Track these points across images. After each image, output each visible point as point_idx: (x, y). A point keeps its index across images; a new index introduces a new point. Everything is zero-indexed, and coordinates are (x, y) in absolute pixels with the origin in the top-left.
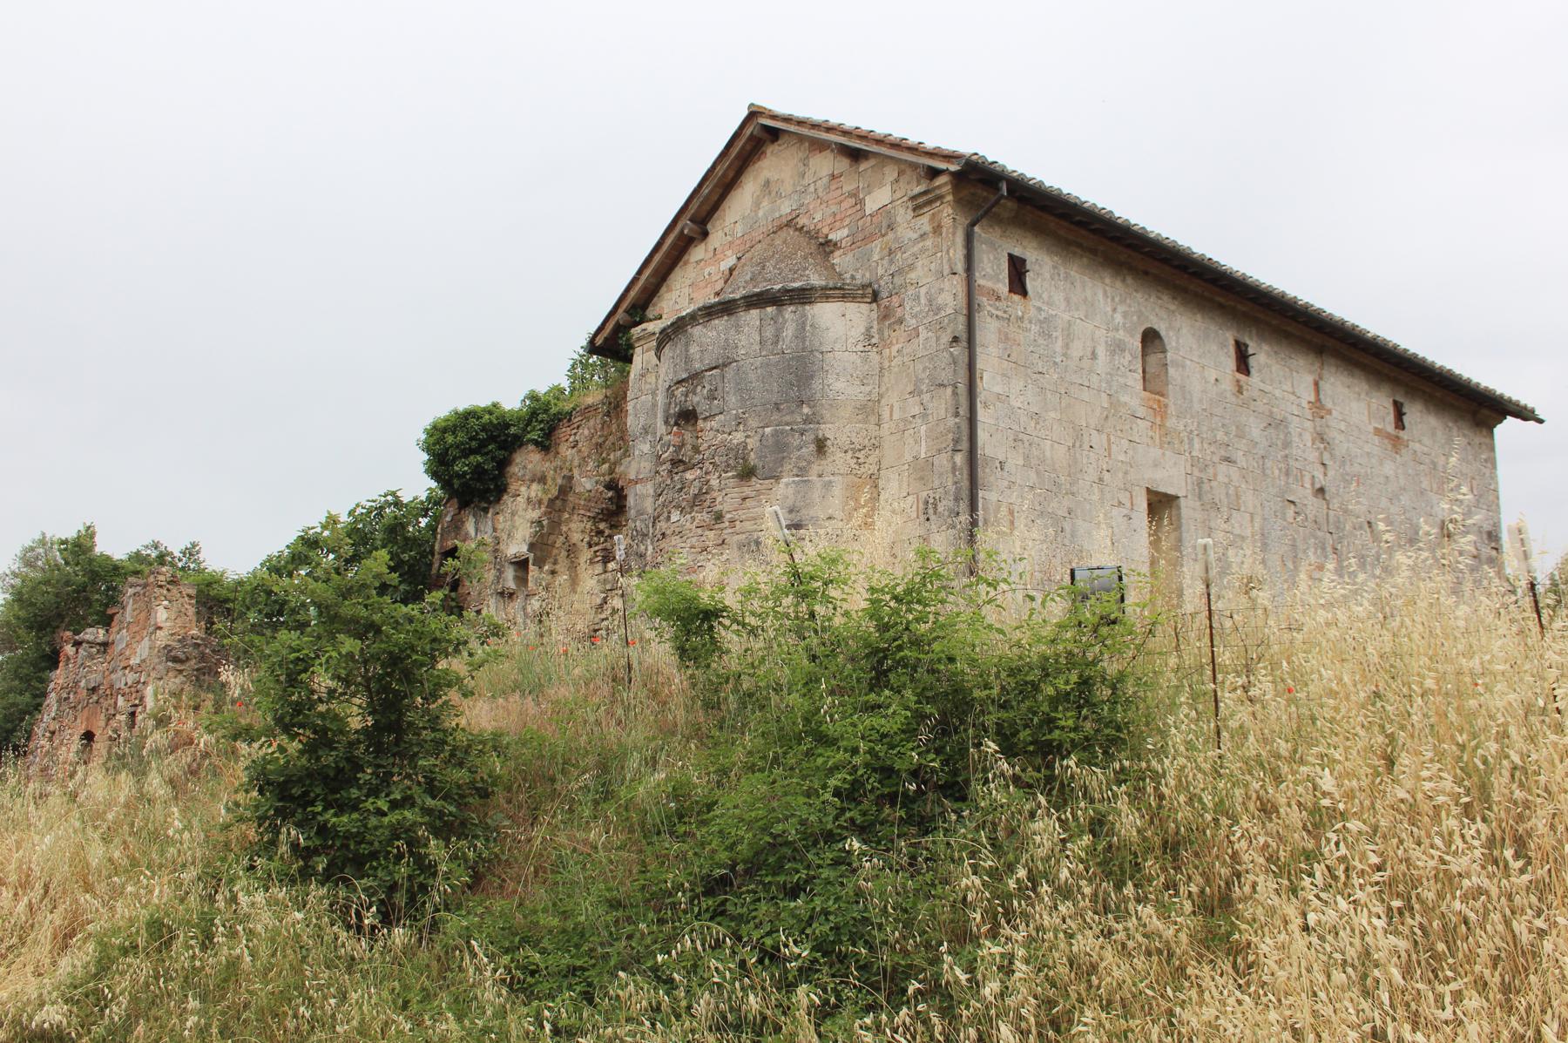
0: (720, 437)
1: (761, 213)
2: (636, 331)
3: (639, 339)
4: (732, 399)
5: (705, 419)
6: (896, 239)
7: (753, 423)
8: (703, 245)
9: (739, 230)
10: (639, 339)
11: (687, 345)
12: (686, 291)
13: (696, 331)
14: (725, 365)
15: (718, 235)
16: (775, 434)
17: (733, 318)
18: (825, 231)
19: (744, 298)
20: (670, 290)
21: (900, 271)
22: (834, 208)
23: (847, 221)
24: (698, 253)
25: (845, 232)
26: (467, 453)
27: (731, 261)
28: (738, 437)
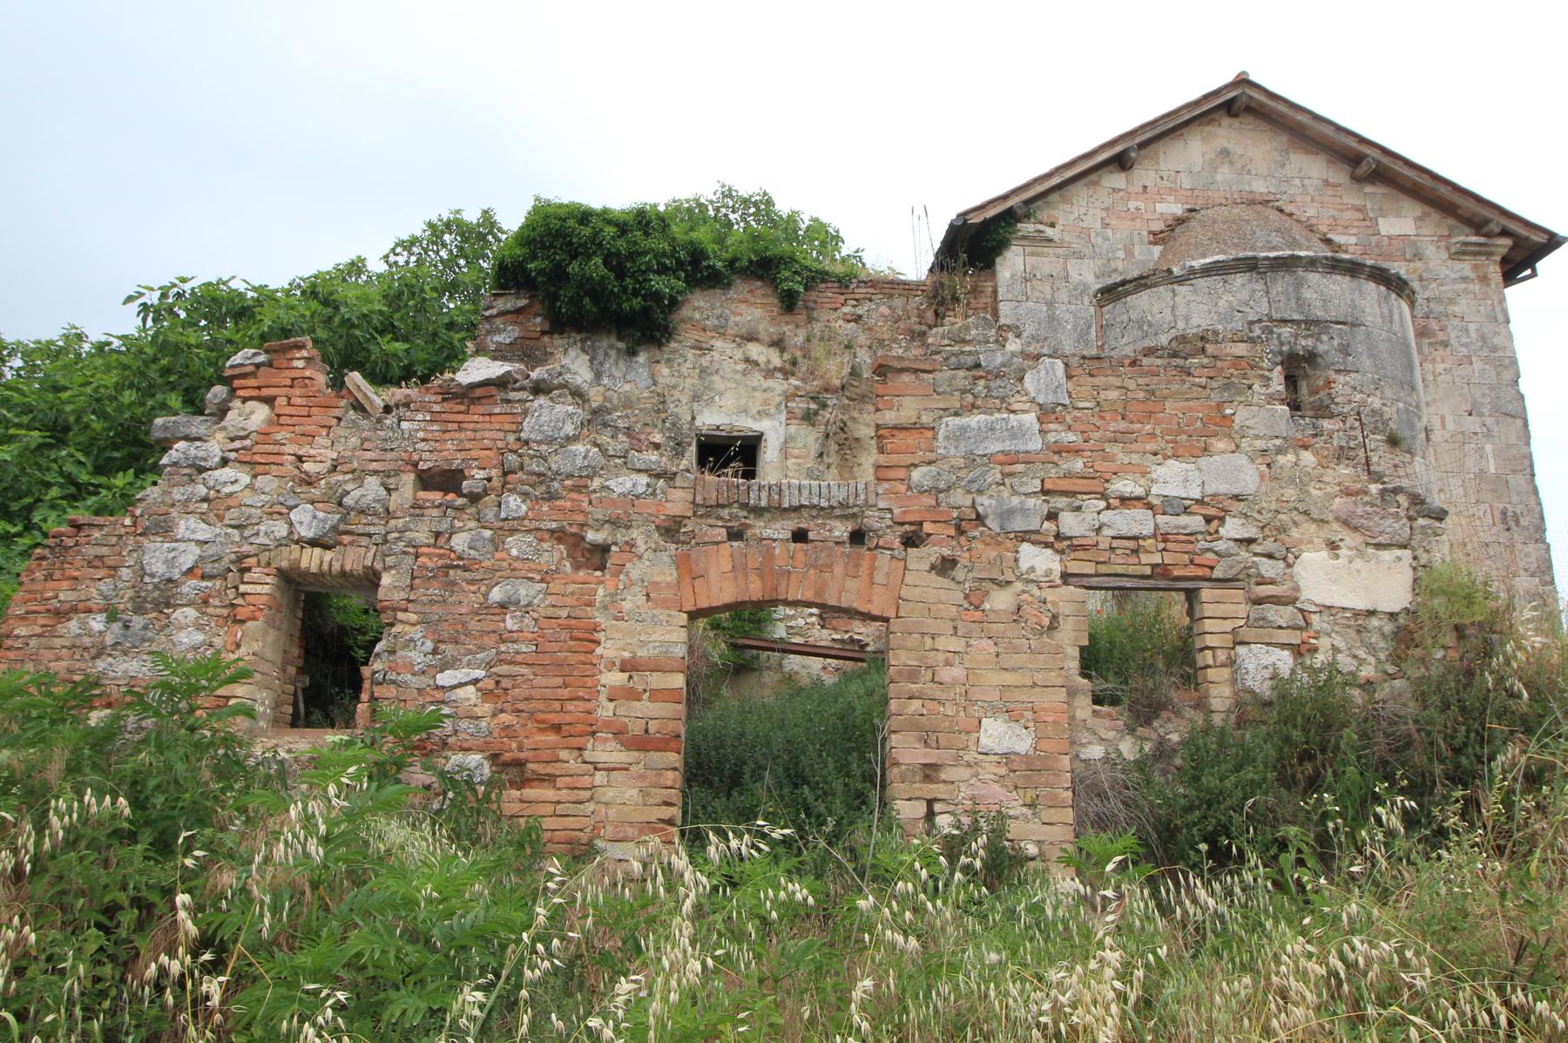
0: (1358, 397)
1: (1219, 177)
2: (1026, 227)
3: (1024, 238)
4: (1367, 363)
5: (1338, 371)
6: (1427, 269)
7: (1389, 393)
8: (1123, 175)
9: (1186, 181)
10: (1024, 238)
11: (1298, 285)
12: (1100, 214)
13: (1313, 278)
14: (1353, 325)
15: (1144, 175)
16: (1407, 411)
17: (1355, 283)
18: (1323, 228)
19: (1372, 267)
20: (1065, 201)
21: (1438, 300)
22: (1333, 212)
23: (1355, 231)
24: (1116, 180)
25: (1353, 240)
26: (663, 270)
27: (1178, 210)
28: (1376, 402)
